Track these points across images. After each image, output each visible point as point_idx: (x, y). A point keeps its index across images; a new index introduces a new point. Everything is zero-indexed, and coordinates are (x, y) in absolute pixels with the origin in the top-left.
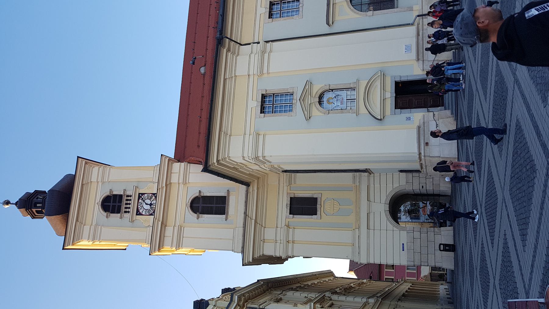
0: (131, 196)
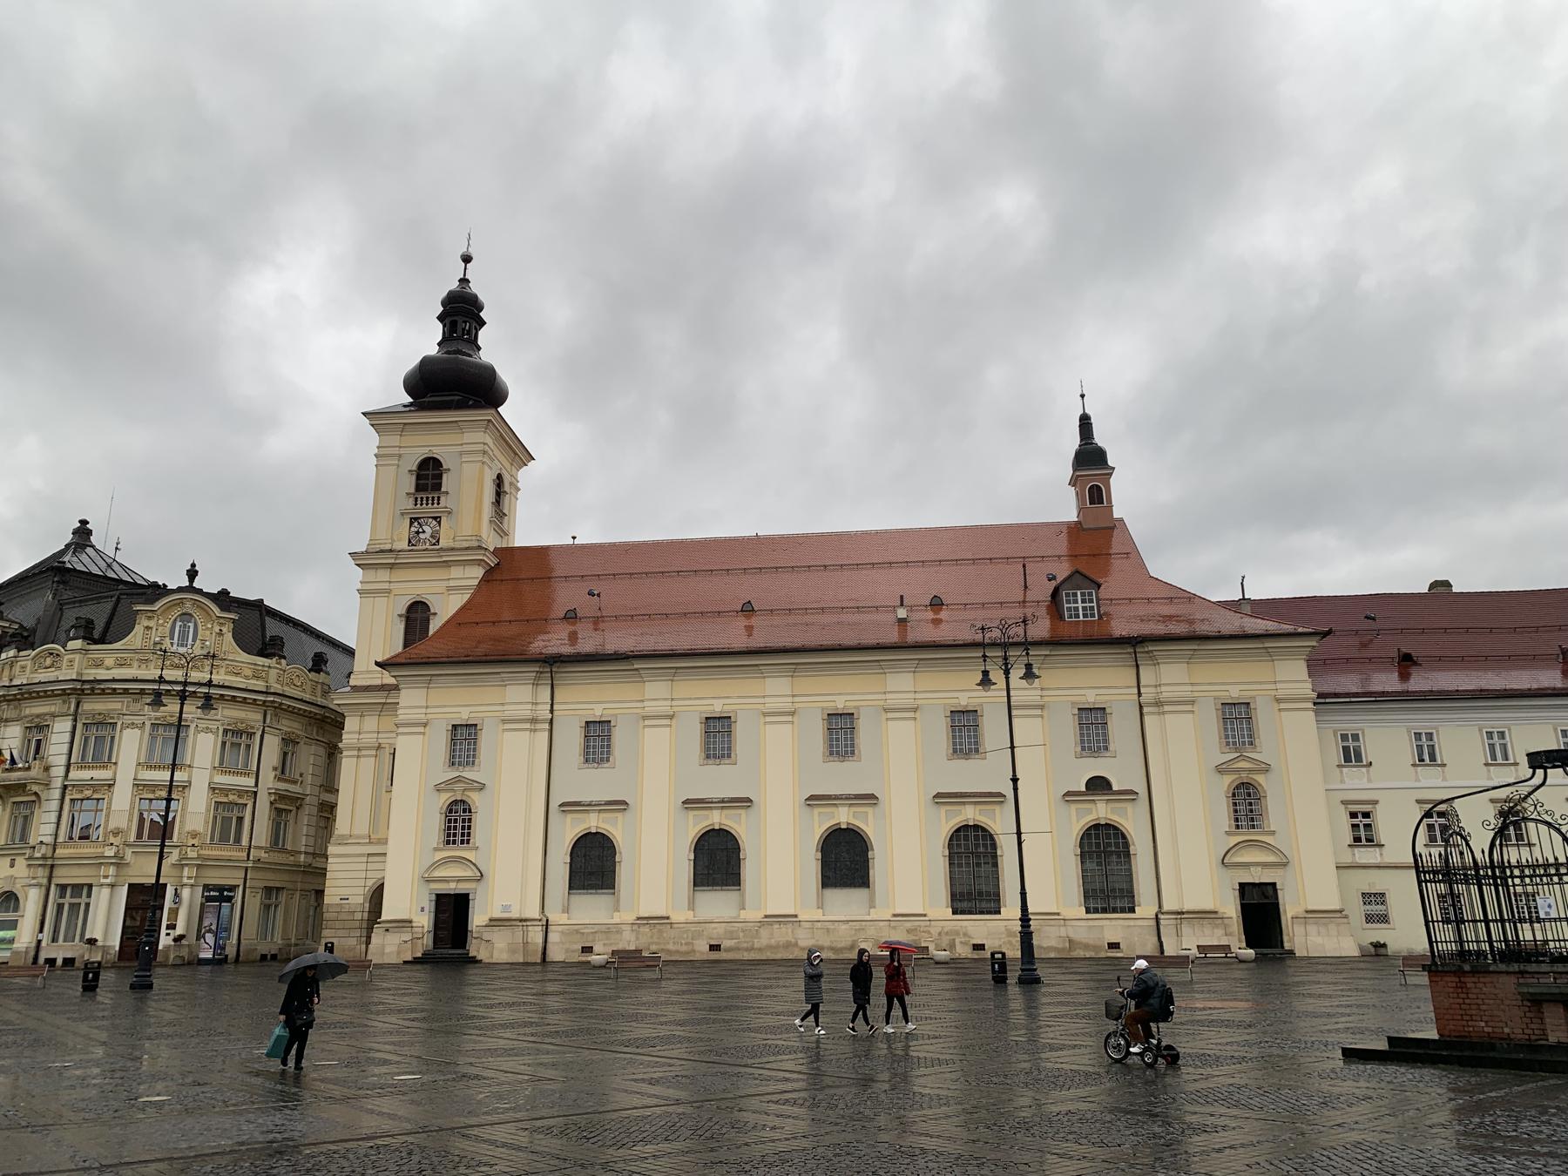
0: (438, 504)
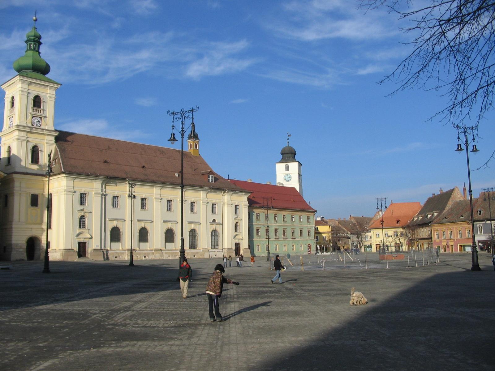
0: (40, 113)
